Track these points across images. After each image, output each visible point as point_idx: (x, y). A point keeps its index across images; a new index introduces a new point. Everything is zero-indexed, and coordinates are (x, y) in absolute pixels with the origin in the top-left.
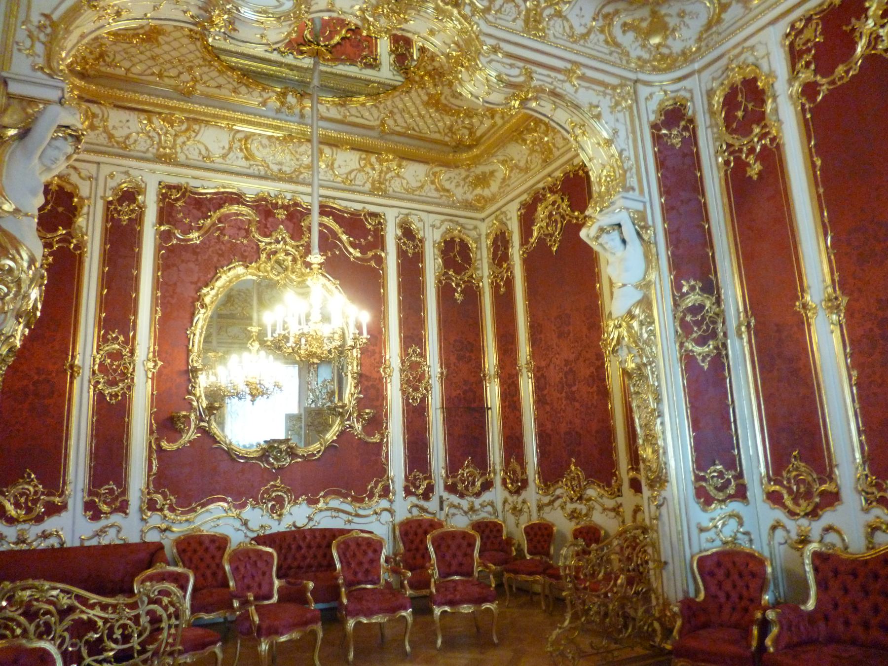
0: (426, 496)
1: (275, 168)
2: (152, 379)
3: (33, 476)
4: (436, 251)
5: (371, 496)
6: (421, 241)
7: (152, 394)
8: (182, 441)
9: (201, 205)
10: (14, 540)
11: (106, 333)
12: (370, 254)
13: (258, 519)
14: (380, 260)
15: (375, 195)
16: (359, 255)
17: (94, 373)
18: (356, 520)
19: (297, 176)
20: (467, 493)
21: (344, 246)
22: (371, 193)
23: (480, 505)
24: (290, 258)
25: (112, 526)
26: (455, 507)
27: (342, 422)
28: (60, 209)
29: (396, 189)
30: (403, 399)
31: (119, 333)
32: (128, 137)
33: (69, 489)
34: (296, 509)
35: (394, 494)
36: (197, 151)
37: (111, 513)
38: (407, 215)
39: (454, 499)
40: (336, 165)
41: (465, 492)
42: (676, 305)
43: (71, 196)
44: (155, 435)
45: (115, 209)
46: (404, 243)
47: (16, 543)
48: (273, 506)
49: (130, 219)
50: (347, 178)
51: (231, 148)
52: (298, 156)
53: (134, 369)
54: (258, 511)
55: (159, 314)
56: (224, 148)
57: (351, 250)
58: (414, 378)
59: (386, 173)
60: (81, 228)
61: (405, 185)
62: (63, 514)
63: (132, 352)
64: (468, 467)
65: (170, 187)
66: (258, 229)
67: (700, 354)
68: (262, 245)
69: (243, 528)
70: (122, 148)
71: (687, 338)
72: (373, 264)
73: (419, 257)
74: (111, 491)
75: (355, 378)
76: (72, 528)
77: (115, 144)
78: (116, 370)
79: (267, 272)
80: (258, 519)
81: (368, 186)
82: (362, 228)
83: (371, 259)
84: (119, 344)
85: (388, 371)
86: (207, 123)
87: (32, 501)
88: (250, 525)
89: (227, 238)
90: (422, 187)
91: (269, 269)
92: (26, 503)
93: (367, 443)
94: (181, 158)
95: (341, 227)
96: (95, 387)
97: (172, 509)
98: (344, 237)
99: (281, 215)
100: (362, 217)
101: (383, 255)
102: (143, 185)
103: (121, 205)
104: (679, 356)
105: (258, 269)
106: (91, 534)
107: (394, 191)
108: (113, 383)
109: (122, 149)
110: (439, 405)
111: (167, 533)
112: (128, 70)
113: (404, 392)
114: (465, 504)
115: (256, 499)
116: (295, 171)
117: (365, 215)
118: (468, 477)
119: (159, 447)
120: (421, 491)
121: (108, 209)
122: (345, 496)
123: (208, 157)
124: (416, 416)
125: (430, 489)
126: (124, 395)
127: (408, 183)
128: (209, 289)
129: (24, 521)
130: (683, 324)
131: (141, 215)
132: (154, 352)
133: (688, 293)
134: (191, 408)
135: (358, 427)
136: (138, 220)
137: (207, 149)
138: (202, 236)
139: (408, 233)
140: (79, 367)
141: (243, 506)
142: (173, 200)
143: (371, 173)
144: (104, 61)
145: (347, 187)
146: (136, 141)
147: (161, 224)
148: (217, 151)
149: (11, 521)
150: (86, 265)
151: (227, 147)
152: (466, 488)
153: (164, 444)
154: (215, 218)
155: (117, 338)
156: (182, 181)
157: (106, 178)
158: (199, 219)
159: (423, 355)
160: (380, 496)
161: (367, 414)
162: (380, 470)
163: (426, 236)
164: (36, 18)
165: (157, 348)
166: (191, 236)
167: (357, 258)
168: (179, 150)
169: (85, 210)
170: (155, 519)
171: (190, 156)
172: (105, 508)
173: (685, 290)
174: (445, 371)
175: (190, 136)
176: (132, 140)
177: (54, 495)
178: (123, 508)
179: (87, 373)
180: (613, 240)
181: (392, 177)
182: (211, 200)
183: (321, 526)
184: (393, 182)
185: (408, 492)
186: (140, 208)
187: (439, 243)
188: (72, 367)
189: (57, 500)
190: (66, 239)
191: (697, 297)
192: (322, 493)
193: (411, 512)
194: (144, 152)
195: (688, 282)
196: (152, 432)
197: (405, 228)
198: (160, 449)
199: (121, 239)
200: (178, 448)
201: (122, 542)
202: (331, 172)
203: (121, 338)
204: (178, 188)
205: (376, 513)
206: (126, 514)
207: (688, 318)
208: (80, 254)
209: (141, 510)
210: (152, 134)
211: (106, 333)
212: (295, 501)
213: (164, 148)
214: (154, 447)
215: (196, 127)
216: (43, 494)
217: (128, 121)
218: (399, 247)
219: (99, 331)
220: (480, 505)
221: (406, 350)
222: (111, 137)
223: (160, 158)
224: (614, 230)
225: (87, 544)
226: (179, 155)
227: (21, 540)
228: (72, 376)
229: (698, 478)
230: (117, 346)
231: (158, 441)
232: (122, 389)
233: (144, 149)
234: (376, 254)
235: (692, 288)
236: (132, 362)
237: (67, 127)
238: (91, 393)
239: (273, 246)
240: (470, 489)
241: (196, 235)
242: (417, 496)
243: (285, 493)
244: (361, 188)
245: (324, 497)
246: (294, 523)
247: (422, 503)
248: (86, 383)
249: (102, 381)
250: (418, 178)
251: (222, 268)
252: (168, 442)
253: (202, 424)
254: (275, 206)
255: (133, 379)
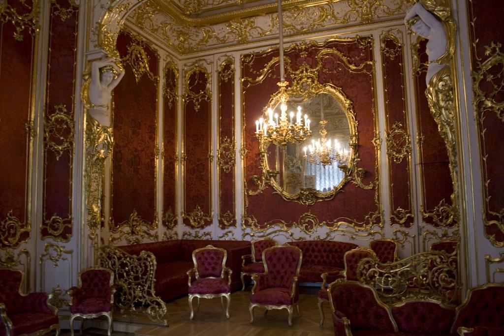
0: (407, 224)
1: (299, 27)
2: (244, 159)
3: (199, 208)
4: (413, 51)
5: (367, 223)
6: (400, 47)
7: (244, 167)
8: (259, 191)
9: (259, 61)
10: (194, 235)
11: (223, 138)
12: (362, 66)
13: (298, 232)
14: (370, 68)
15: (364, 24)
16: (355, 68)
17: (219, 159)
18: (357, 238)
19: (312, 28)
20: (442, 224)
21: (344, 63)
22: (361, 24)
23: (453, 233)
24: (310, 80)
25: (230, 232)
26: (432, 234)
27: (346, 177)
28: (201, 82)
29: (380, 16)
30: (389, 159)
31: (228, 138)
32: (225, 37)
33: (212, 213)
34: (319, 229)
35: (384, 223)
36: (257, 32)
37: (229, 226)
38: (389, 31)
39: (430, 228)
40: (335, 13)
41: (440, 223)
42: (476, 68)
43: (204, 74)
44: (247, 188)
45: (222, 75)
46: (387, 52)
47: (195, 237)
48: (306, 226)
49: (229, 79)
50: (344, 19)
51: (273, 24)
52: (311, 16)
53: (235, 155)
54: (298, 229)
55: (245, 125)
56: (269, 26)
57: (351, 66)
58: (397, 143)
59: (371, 7)
60: (209, 89)
61: (386, 10)
62: (211, 225)
63: (234, 146)
64: (442, 205)
65: (246, 56)
66: (291, 67)
67: (499, 109)
68: (292, 76)
69: (291, 238)
70: (224, 43)
71: (486, 96)
72: (365, 71)
73: (400, 58)
74: (229, 215)
75: (353, 149)
76: (214, 231)
77: (221, 43)
78: (227, 158)
79: (298, 91)
80: (298, 232)
81: (359, 20)
82: (357, 50)
83: (364, 68)
84: (228, 143)
85: (378, 141)
86: (258, 15)
87: (200, 218)
88: (294, 236)
89: (275, 76)
90: (400, 8)
91: (298, 89)
92: (197, 220)
93: (363, 189)
94: (250, 39)
95: (341, 52)
96: (219, 165)
97: (256, 226)
98: (344, 59)
99: (304, 55)
100: (356, 42)
101: (371, 63)
102: (233, 59)
103: (224, 73)
104: (475, 113)
105: (292, 90)
106: (221, 235)
107: (378, 17)
108: (226, 163)
109: (223, 43)
110: (418, 161)
111: (254, 237)
112: (212, 4)
113: (389, 155)
114: (440, 232)
115: (297, 223)
116: (311, 25)
117: (358, 40)
118: (442, 213)
119: (248, 193)
120: (403, 221)
121: (219, 76)
122: (351, 223)
123: (263, 33)
124: (399, 171)
125: (410, 220)
126: (231, 168)
127: (388, 8)
128: (266, 107)
129: (198, 228)
130: (483, 85)
131: (234, 75)
132: (244, 145)
133: (490, 56)
134: (260, 173)
135: (358, 181)
136: (232, 79)
137: (262, 29)
138: (263, 79)
139: (390, 44)
140: (213, 157)
141: (289, 226)
142: (248, 63)
143: (360, 10)
144: (202, 5)
145: (345, 24)
146: (228, 37)
147: (242, 78)
148: (266, 28)
149: (193, 227)
150: (212, 106)
151: (271, 24)
152: (441, 221)
153: (251, 193)
154: (268, 68)
155: (227, 141)
156: (251, 51)
157: (217, 61)
158: (260, 69)
159: (404, 128)
160: (373, 223)
161: (360, 171)
162: (374, 207)
163: (405, 42)
164: (95, 25)
165: (245, 143)
166: (257, 80)
167: (354, 70)
168: (248, 34)
169: (210, 79)
170: (248, 230)
171: (254, 36)
172: (226, 223)
173: (488, 53)
174: (423, 138)
175: (251, 25)
176: (227, 38)
177: (207, 216)
178: (234, 224)
179: (215, 159)
180: (419, 28)
181: (376, 8)
182: (266, 57)
183: (335, 240)
184: (376, 11)
185: (393, 221)
186: (232, 71)
187: (416, 44)
188: (210, 156)
189: (208, 219)
190: (204, 96)
191: (498, 57)
192: (335, 221)
193: (395, 235)
194: (232, 42)
195: (490, 46)
196: (245, 187)
197: (387, 41)
198: (249, 196)
199: (226, 89)
200: (257, 195)
201: (234, 240)
202: (333, 19)
203: (229, 140)
204: (249, 55)
205: (370, 234)
206: (236, 227)
207: (490, 78)
208: (210, 101)
209: (242, 225)
210: (235, 31)
211: (223, 138)
212: (319, 224)
213: (240, 37)
214: (246, 193)
215: (252, 20)
216: (203, 216)
217: (222, 29)
218: (383, 55)
219: (219, 138)
220: (453, 233)
221: (391, 126)
222: (218, 39)
223: (239, 43)
224: (417, 20)
225: (221, 239)
226: (249, 37)
227: (197, 236)
228: (211, 161)
229: (489, 217)
230: (227, 144)
231: (248, 191)
232: (231, 165)
233: (233, 40)
234: (367, 64)
235: (494, 50)
236: (234, 152)
237: (105, 67)
238: (218, 169)
239: (300, 75)
240: (444, 221)
241: (262, 77)
242: (400, 224)
243: (313, 219)
244: (354, 23)
245: (337, 222)
246: (319, 236)
247: (404, 229)
248: (216, 164)
249: (222, 162)
250: (395, 2)
251: (273, 94)
252: (253, 191)
253: (267, 181)
254: (301, 50)
255: (235, 160)
